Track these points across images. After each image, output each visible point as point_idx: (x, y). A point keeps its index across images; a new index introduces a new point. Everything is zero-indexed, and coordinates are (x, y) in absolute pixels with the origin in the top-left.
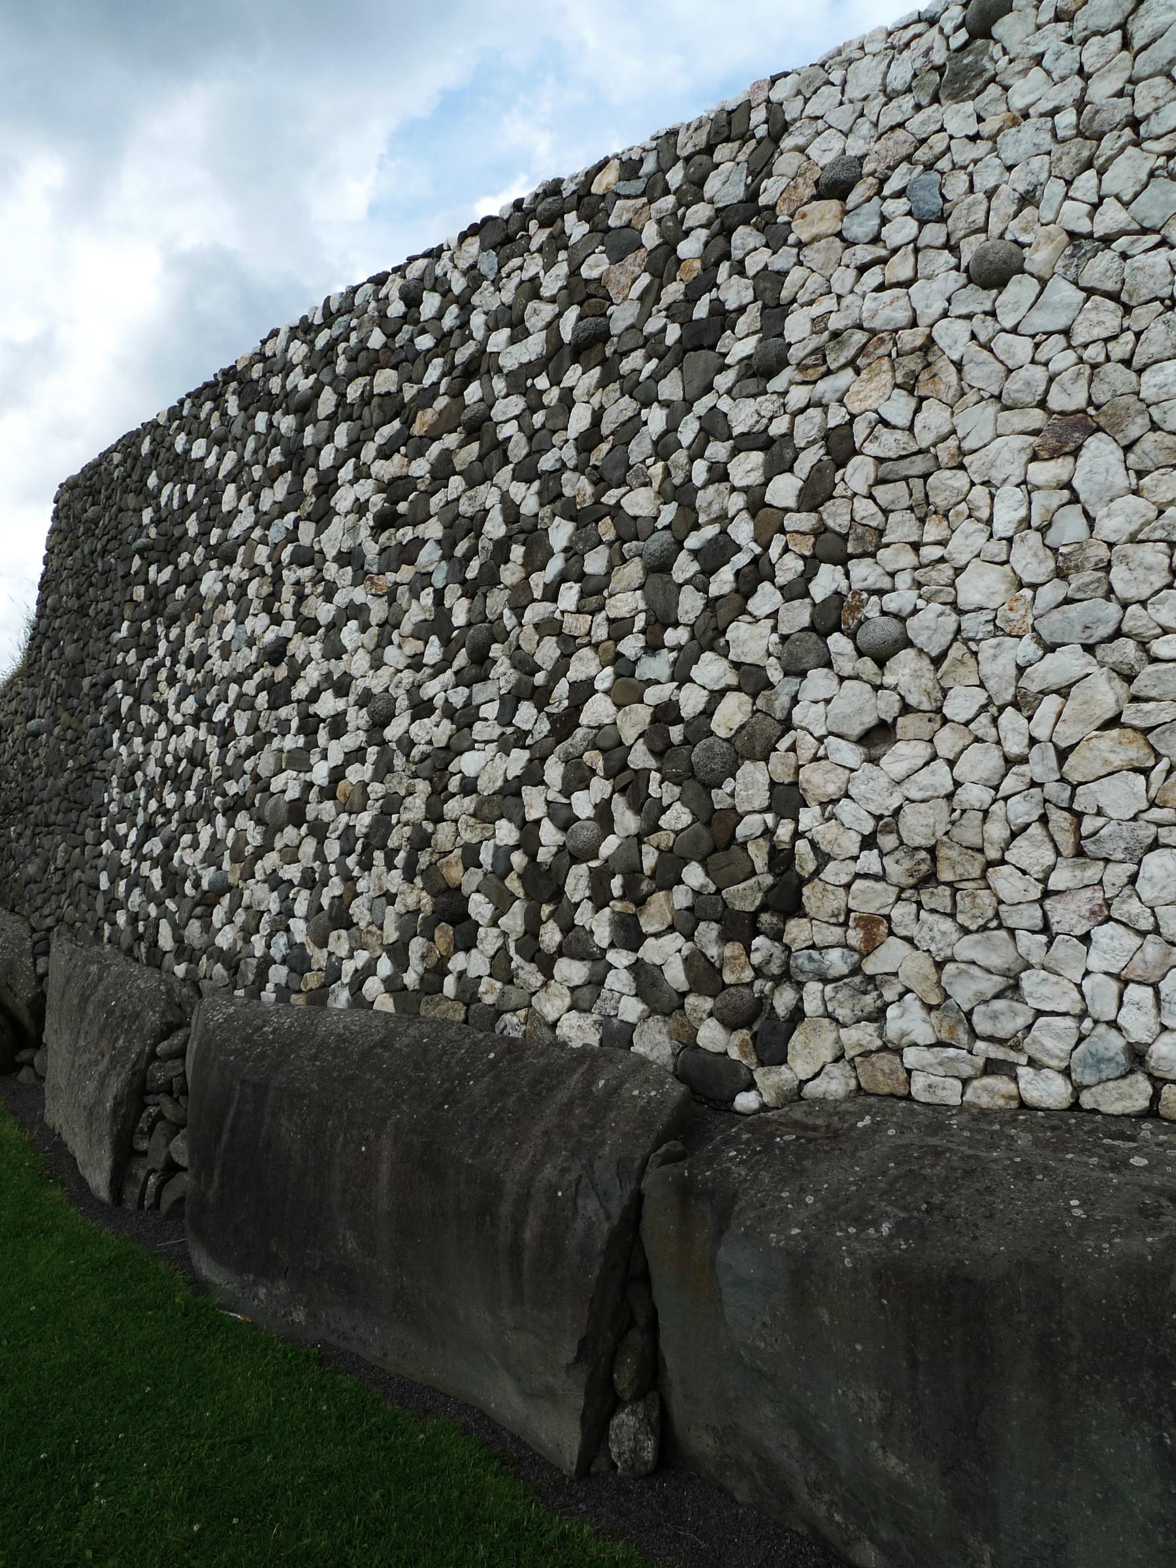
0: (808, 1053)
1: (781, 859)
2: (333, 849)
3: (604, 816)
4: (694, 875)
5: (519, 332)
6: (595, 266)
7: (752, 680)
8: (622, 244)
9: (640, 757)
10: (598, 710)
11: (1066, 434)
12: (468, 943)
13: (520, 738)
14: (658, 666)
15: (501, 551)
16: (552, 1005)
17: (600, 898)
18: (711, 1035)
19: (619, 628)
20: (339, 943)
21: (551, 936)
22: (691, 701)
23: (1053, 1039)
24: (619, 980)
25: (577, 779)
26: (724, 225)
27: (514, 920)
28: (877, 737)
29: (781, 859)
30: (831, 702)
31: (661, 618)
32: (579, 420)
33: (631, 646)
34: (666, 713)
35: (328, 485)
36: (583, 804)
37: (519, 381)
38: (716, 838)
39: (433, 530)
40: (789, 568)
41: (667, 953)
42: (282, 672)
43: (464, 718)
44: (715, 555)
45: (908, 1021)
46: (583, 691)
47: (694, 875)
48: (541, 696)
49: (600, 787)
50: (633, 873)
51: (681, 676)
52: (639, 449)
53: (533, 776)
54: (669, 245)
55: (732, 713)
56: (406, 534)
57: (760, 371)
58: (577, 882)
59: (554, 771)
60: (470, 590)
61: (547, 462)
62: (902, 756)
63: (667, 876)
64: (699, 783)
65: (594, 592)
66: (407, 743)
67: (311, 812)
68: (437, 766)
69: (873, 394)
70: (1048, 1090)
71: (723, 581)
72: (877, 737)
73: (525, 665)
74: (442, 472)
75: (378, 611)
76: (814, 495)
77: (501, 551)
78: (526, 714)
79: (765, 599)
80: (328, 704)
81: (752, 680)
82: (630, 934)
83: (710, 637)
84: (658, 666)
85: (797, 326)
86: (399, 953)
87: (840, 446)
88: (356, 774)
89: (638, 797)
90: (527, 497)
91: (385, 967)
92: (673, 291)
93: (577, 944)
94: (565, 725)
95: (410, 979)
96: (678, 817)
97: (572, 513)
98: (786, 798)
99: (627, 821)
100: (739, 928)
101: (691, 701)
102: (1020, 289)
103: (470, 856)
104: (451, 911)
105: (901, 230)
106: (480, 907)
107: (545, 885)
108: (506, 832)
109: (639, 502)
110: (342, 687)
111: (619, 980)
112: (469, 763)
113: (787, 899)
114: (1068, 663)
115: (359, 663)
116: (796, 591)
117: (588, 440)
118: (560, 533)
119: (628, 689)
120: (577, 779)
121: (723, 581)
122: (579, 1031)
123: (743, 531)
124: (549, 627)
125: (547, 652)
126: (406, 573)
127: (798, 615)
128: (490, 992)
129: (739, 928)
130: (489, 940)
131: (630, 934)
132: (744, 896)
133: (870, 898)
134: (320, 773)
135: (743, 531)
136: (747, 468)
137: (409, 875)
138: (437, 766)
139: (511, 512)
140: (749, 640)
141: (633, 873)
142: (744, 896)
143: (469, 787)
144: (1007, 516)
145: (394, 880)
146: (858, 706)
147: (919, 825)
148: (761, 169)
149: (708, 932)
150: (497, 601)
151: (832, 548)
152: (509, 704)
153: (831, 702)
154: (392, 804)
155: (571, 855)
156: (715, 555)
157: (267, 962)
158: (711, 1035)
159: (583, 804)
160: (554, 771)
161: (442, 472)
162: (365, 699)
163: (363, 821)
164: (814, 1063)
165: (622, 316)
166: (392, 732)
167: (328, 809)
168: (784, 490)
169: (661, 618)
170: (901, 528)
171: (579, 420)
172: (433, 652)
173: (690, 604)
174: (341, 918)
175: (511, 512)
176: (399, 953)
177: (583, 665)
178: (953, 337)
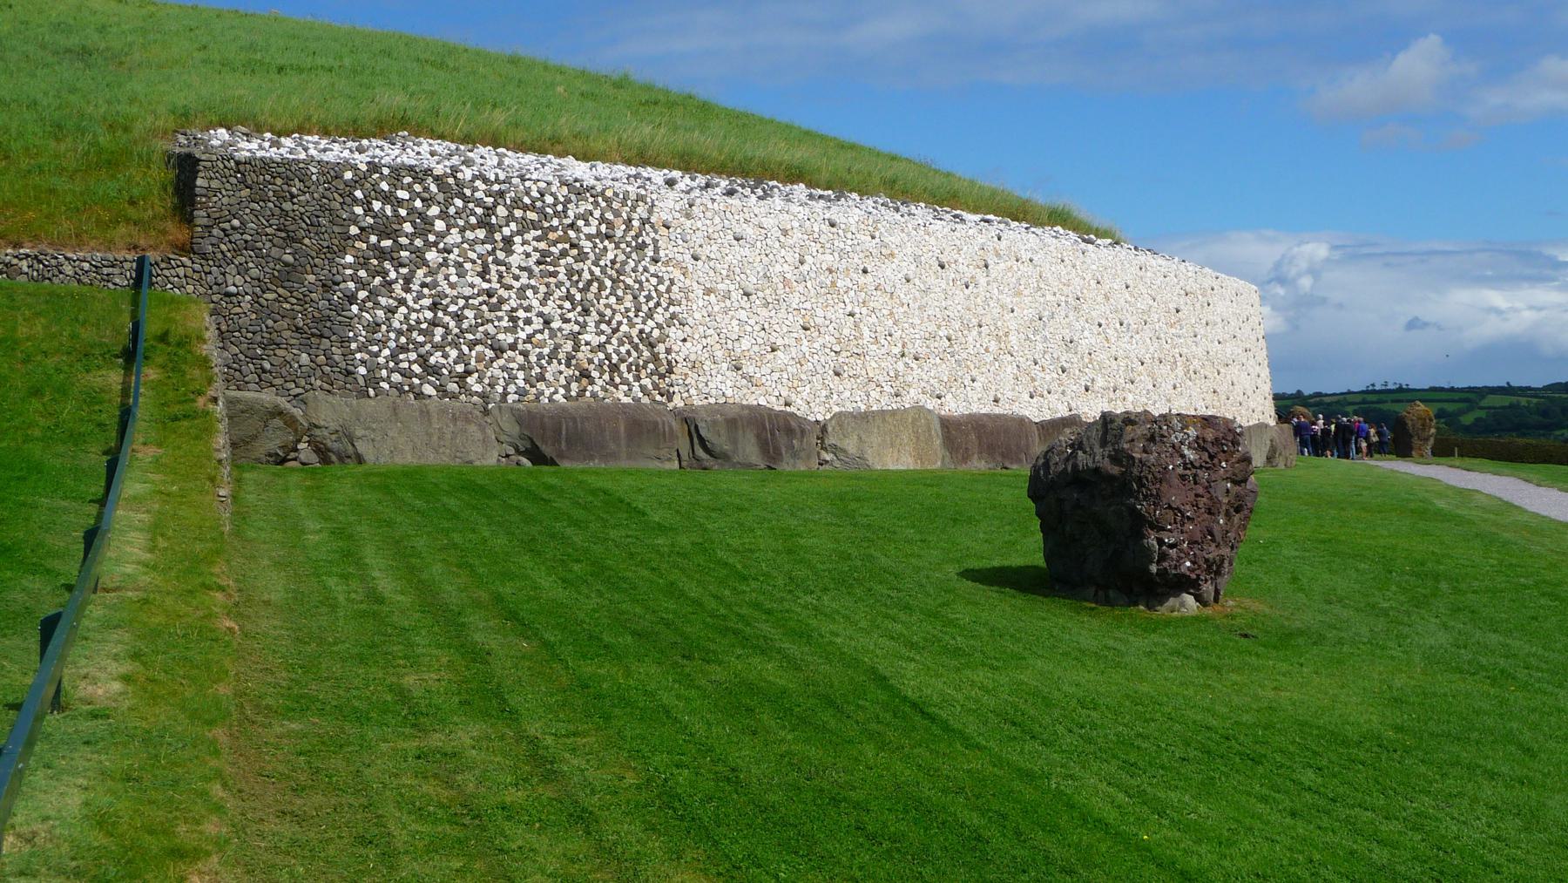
0: (677, 399)
1: (669, 363)
2: (533, 359)
3: (628, 352)
4: (651, 366)
5: (587, 224)
6: (609, 215)
7: (659, 326)
8: (617, 214)
9: (636, 340)
10: (624, 328)
11: (708, 291)
12: (592, 383)
13: (603, 332)
14: (639, 320)
15: (589, 283)
16: (621, 395)
17: (629, 371)
18: (658, 398)
19: (627, 310)
20: (541, 386)
21: (617, 380)
22: (647, 330)
23: (714, 392)
24: (636, 388)
25: (621, 343)
26: (644, 222)
27: (606, 377)
28: (684, 340)
29: (669, 363)
30: (675, 333)
31: (638, 310)
32: (610, 255)
33: (631, 314)
34: (641, 331)
35: (508, 241)
36: (623, 350)
37: (589, 237)
38: (655, 358)
39: (562, 270)
40: (664, 305)
41: (646, 382)
42: (494, 300)
43: (584, 326)
44: (649, 298)
45: (693, 391)
46: (620, 323)
47: (651, 366)
48: (609, 323)
49: (627, 346)
50: (637, 366)
51: (644, 323)
52: (628, 268)
53: (608, 342)
54: (630, 220)
55: (656, 333)
56: (552, 269)
57: (655, 260)
58: (623, 367)
59: (614, 341)
60: (580, 291)
61: (602, 263)
62: (688, 344)
63: (645, 367)
64: (652, 346)
65: (620, 300)
66: (560, 329)
67: (520, 347)
68: (575, 337)
69: (677, 274)
70: (712, 401)
71: (651, 304)
72: (684, 340)
73: (601, 315)
74: (564, 254)
75: (543, 289)
76: (668, 291)
77: (589, 283)
78: (603, 327)
79: (659, 310)
80: (521, 314)
81: (659, 326)
82: (638, 378)
83: (650, 316)
84: (639, 320)
85: (662, 253)
86: (567, 388)
87: (672, 282)
88: (539, 336)
89: (636, 348)
90: (597, 271)
91: (562, 391)
92: (633, 233)
93: (625, 382)
94: (615, 331)
95: (573, 394)
96: (646, 354)
97: (610, 278)
98: (668, 351)
99: (634, 354)
100: (662, 377)
101: (647, 330)
102: (700, 263)
103: (590, 361)
104: (584, 374)
105: (680, 242)
106: (595, 374)
107: (614, 368)
108: (602, 356)
109: (629, 281)
110: (528, 309)
111: (636, 388)
112: (587, 337)
113: (670, 371)
114: (711, 331)
115: (535, 303)
116: (666, 310)
117: (613, 262)
118: (608, 283)
119: (631, 325)
120: (621, 343)
121: (651, 304)
122: (626, 400)
123: (654, 294)
124: (607, 306)
125: (608, 312)
126: (552, 280)
127: (668, 315)
128: (601, 394)
129: (662, 377)
130: (600, 382)
131: (638, 378)
132: (662, 370)
133: (686, 370)
134: (522, 335)
135: (654, 294)
136: (654, 281)
137: (568, 366)
138: (575, 337)
139: (592, 273)
140: (659, 318)
141: (637, 366)
142: (662, 370)
143: (587, 344)
144: (701, 303)
145: (563, 367)
146: (681, 335)
147: (693, 357)
148: (650, 212)
149: (655, 378)
150: (590, 296)
151: (671, 303)
152: (598, 324)
153: (675, 333)
154: (557, 347)
155: (623, 361)
156: (649, 298)
157: (505, 394)
158: (658, 398)
159: (623, 350)
160: (614, 341)
161: (564, 254)
162: (540, 314)
163: (546, 351)
164: (678, 402)
165: (619, 233)
166: (553, 325)
167: (529, 346)
168: (662, 288)
169: (638, 310)
170: (684, 302)
171: (610, 255)
172: (567, 305)
173: (645, 308)
174: (541, 378)
175: (592, 273)
176: (567, 388)
177: (618, 317)
178: (690, 268)
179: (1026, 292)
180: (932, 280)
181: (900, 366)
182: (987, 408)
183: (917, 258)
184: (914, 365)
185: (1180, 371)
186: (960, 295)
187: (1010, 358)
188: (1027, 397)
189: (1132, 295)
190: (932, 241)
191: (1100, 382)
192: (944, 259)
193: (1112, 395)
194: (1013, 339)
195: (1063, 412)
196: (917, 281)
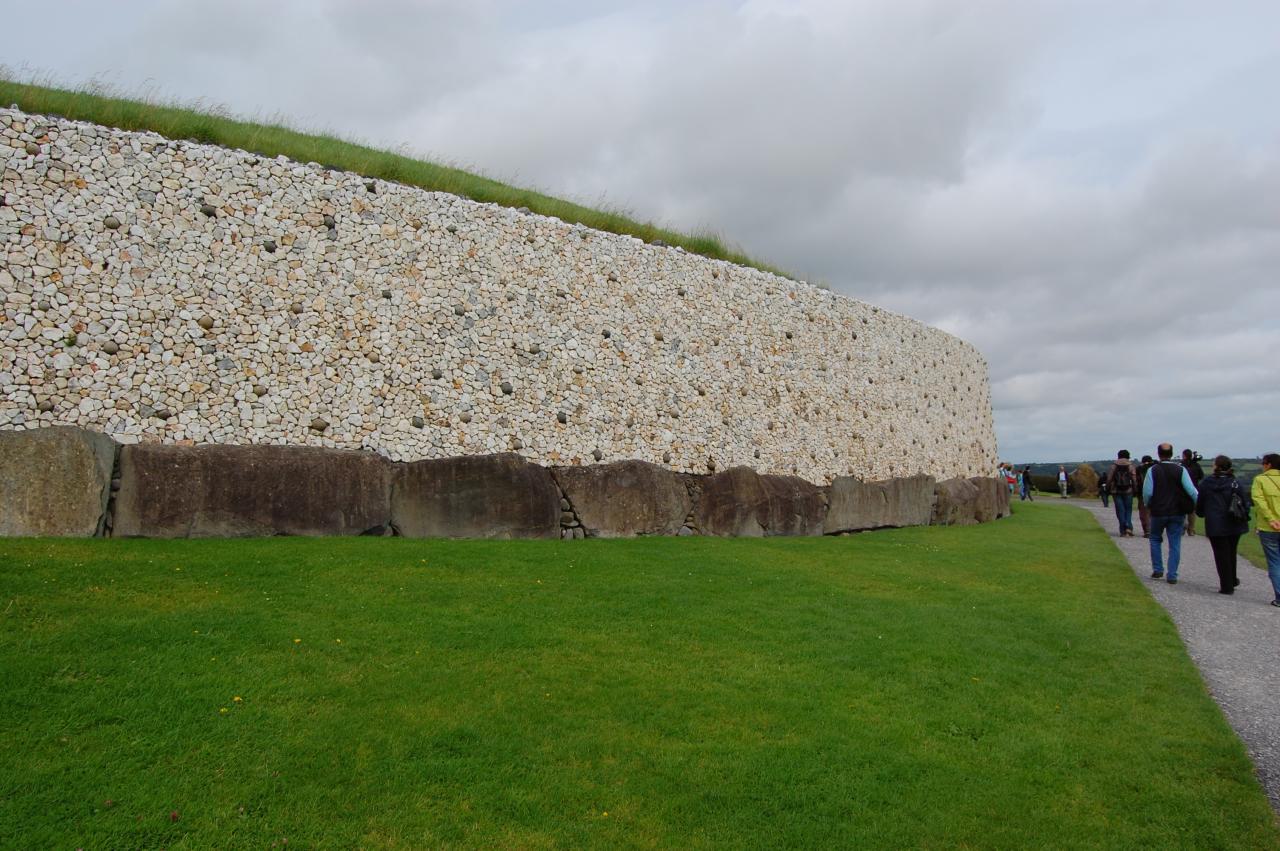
179: (430, 273)
180: (176, 229)
181: (63, 361)
182: (297, 436)
183: (144, 197)
184: (102, 362)
185: (786, 406)
186: (250, 261)
187: (367, 364)
188: (405, 424)
189: (688, 303)
190: (193, 172)
191: (596, 410)
192: (212, 200)
193: (621, 429)
194: (383, 338)
195: (494, 445)
196: (137, 230)
